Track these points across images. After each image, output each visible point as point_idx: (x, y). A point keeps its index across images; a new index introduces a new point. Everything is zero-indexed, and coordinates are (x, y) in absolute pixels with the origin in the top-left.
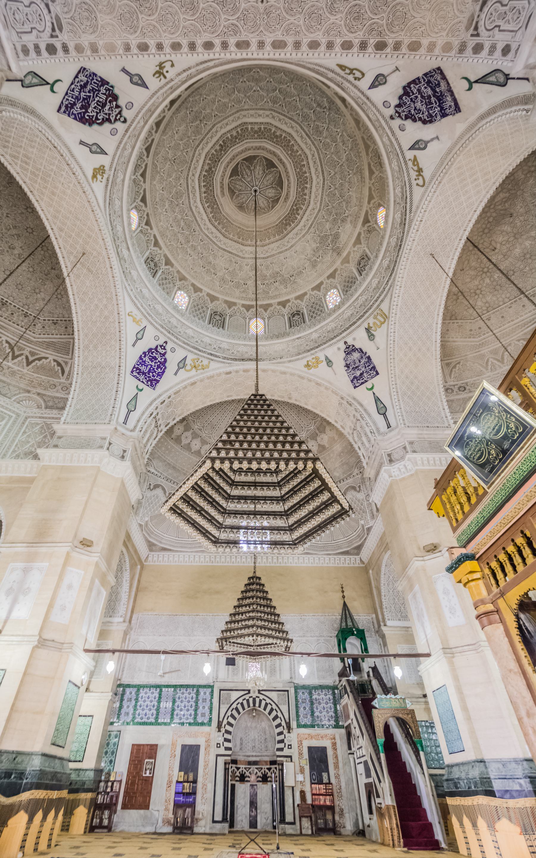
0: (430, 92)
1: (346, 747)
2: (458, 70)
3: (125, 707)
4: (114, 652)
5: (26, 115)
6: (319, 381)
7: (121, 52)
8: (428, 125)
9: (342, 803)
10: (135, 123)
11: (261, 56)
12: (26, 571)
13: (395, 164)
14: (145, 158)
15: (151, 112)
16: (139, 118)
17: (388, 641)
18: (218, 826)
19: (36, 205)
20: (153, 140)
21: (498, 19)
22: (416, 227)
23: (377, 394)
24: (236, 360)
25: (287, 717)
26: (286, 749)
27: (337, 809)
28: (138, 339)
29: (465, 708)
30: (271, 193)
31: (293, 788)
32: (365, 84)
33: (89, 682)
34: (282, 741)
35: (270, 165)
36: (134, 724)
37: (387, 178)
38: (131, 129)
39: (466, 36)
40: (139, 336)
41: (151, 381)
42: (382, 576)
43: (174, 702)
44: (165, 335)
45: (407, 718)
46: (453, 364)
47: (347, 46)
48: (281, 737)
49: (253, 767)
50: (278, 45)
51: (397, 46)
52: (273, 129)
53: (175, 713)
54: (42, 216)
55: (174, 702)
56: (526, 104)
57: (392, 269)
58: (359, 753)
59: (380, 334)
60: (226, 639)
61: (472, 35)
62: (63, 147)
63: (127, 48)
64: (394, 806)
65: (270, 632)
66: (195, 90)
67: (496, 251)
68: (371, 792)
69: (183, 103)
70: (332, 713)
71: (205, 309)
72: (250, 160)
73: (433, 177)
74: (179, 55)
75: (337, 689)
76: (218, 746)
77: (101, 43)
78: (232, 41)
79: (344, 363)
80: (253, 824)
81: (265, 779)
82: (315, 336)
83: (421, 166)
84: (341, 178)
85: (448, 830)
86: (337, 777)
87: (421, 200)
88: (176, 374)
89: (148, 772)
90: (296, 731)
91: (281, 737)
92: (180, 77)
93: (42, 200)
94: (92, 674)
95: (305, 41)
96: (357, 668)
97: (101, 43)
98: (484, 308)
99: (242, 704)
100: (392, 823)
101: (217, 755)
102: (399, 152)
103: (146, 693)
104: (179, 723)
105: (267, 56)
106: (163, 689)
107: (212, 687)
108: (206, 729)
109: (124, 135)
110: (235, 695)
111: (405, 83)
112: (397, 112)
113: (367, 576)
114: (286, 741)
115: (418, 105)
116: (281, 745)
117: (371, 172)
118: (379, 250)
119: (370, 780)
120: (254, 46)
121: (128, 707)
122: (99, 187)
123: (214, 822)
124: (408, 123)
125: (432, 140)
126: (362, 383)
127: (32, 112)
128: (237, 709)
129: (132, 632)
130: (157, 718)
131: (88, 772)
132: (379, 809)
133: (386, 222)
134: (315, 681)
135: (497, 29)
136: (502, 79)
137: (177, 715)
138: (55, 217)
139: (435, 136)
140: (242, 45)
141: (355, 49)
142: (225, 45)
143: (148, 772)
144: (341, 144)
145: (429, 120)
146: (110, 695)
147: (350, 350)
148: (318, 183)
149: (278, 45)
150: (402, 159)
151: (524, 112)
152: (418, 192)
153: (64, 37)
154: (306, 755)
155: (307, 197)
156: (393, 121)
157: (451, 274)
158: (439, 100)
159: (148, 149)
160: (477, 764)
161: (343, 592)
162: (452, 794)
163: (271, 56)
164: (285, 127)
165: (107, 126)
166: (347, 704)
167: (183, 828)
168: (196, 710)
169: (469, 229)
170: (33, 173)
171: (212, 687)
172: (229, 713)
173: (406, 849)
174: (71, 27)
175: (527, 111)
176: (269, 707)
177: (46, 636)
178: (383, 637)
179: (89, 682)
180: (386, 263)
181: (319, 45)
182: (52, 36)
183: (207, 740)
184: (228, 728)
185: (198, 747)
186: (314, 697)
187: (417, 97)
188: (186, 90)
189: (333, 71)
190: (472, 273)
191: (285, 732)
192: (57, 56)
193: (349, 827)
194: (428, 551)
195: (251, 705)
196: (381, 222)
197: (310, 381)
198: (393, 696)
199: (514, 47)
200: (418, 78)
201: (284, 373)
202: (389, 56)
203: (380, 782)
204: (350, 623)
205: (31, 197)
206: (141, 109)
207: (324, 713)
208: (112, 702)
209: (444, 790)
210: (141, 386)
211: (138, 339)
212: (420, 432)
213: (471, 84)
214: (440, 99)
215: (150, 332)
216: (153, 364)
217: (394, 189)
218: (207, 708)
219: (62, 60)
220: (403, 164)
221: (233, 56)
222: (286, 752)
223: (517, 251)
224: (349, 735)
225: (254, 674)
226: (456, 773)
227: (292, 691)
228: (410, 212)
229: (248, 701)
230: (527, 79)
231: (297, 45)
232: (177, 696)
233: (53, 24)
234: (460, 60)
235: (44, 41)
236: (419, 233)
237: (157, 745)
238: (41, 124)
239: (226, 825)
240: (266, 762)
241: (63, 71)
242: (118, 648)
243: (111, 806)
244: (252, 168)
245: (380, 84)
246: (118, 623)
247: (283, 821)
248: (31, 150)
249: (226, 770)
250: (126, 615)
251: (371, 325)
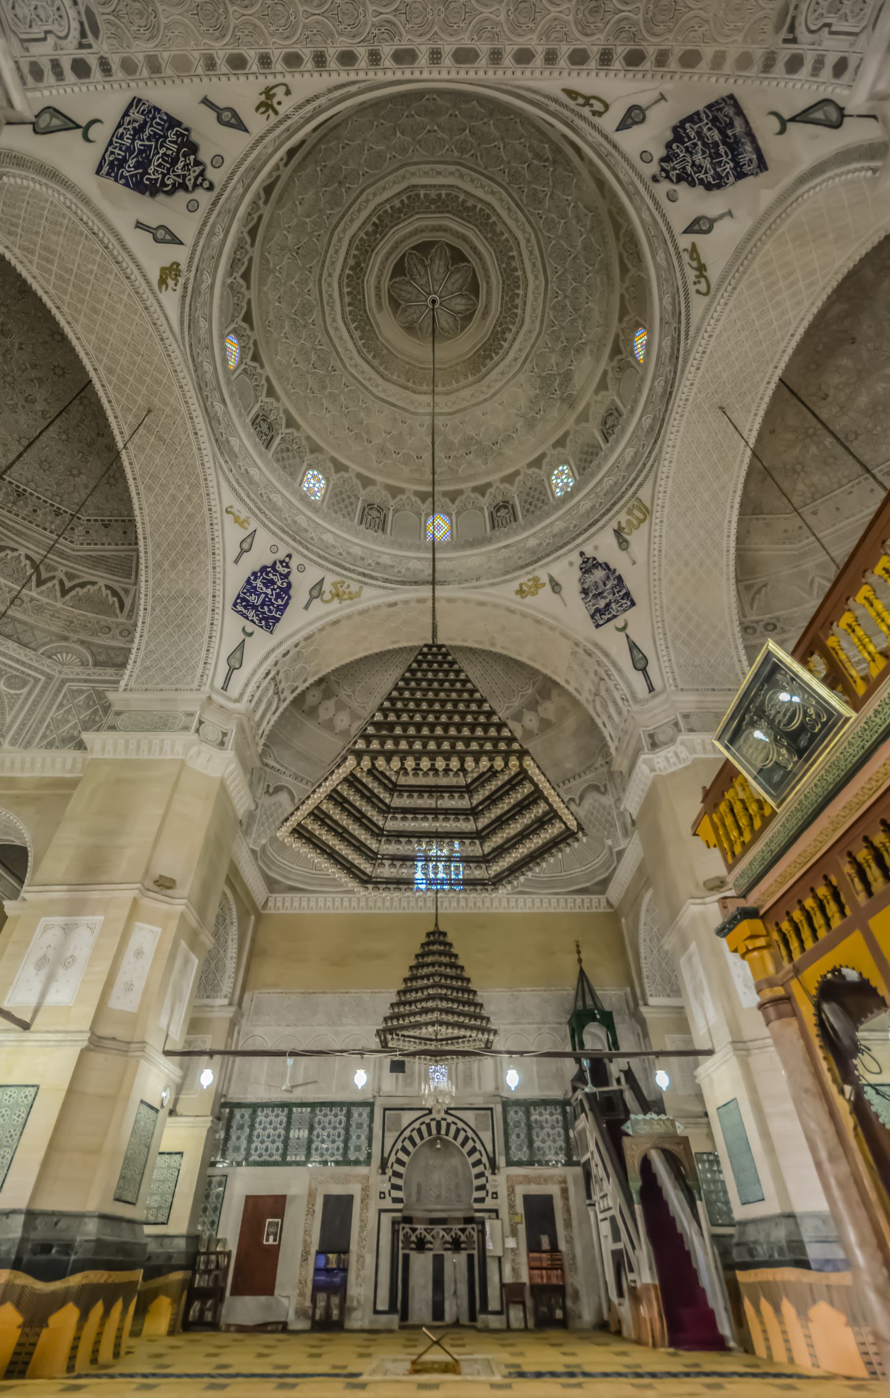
0: (717, 136)
1: (583, 1193)
2: (766, 98)
3: (234, 1138)
4: (211, 1054)
5: (44, 180)
6: (540, 616)
7: (200, 71)
8: (715, 192)
9: (577, 1280)
10: (229, 190)
11: (435, 75)
12: (67, 929)
13: (661, 257)
14: (248, 246)
15: (255, 170)
16: (234, 182)
17: (651, 1030)
18: (384, 1318)
19: (67, 330)
20: (260, 218)
21: (829, 12)
22: (695, 363)
23: (632, 637)
24: (404, 583)
25: (490, 1149)
26: (488, 1200)
27: (569, 1290)
28: (243, 551)
29: (765, 1134)
30: (459, 304)
31: (500, 1259)
32: (610, 121)
33: (176, 1101)
34: (482, 1188)
35: (458, 257)
36: (248, 1165)
37: (649, 281)
38: (221, 201)
39: (775, 41)
40: (246, 546)
41: (266, 619)
42: (642, 927)
43: (311, 1129)
44: (287, 544)
45: (677, 1150)
46: (755, 589)
47: (579, 58)
48: (482, 1181)
49: (438, 1229)
50: (464, 56)
51: (662, 59)
52: (462, 197)
53: (314, 1146)
54: (79, 349)
55: (311, 1129)
56: (873, 158)
57: (656, 431)
58: (603, 1204)
59: (637, 539)
60: (391, 1031)
61: (786, 41)
62: (108, 234)
63: (210, 64)
64: (655, 1286)
65: (461, 1019)
66: (329, 131)
67: (829, 399)
68: (620, 1262)
69: (310, 152)
70: (561, 1143)
71: (353, 499)
72: (424, 248)
73: (723, 279)
74: (297, 76)
75: (570, 1104)
76: (382, 1195)
77: (165, 56)
78: (387, 50)
79: (578, 587)
80: (438, 1312)
81: (456, 1245)
82: (532, 542)
83: (703, 261)
84: (574, 280)
85: (739, 1319)
86: (570, 1241)
87: (703, 318)
88: (306, 607)
89: (271, 1238)
90: (505, 1172)
91: (482, 1181)
92: (302, 112)
93: (77, 321)
94: (179, 1089)
95: (509, 50)
96: (599, 1074)
97: (166, 55)
98: (809, 495)
99: (419, 1131)
100: (651, 1311)
101: (381, 1211)
102: (667, 236)
103: (267, 1116)
104: (320, 1162)
105: (447, 76)
106: (294, 1110)
107: (371, 1105)
108: (363, 1170)
109: (211, 211)
110: (407, 1117)
111: (675, 122)
112: (663, 169)
113: (615, 930)
114: (488, 1187)
115: (698, 158)
116: (482, 1194)
117: (624, 269)
118: (636, 401)
119: (619, 1246)
120: (423, 60)
121: (238, 1138)
122: (170, 300)
123: (376, 1312)
124: (682, 189)
125: (721, 217)
126: (609, 620)
127: (53, 175)
128: (411, 1139)
129: (244, 1021)
130: (284, 1155)
131: (176, 1241)
132: (633, 1290)
133: (648, 354)
134: (535, 1093)
135: (826, 29)
136: (834, 116)
137: (317, 1149)
138: (100, 350)
139: (725, 210)
140: (405, 57)
141: (593, 64)
142: (375, 58)
143: (271, 1238)
144: (574, 222)
145: (716, 184)
146: (208, 1121)
147: (589, 565)
148: (537, 288)
149: (464, 56)
150: (672, 250)
151: (870, 173)
152: (698, 304)
153: (102, 46)
154: (520, 1208)
155: (519, 311)
156: (657, 185)
157: (752, 441)
158: (733, 150)
159: (253, 233)
160: (784, 1220)
161: (579, 952)
162: (746, 1266)
163: (453, 75)
164: (479, 190)
165: (181, 197)
166: (584, 1129)
167: (328, 1325)
168: (346, 1142)
169: (782, 365)
170: (60, 277)
171: (371, 1105)
172: (399, 1145)
173: (672, 1350)
174: (113, 30)
175: (874, 170)
176: (462, 1135)
177: (105, 1031)
178: (642, 1022)
179: (176, 1101)
180: (647, 422)
181: (533, 56)
182: (81, 46)
183: (365, 1185)
184: (398, 1168)
185: (350, 1198)
186: (533, 1118)
187: (695, 145)
188: (315, 130)
189: (556, 101)
190: (789, 436)
191: (488, 1173)
192: (92, 79)
193: (588, 1316)
194: (712, 889)
195: (434, 1132)
196: (640, 353)
197: (524, 615)
198: (655, 1116)
199: (852, 63)
200: (697, 113)
201: (482, 604)
202: (649, 76)
203: (634, 1248)
204: (589, 1002)
205: (59, 317)
206: (238, 166)
207: (549, 1141)
208: (212, 1131)
209: (735, 1257)
210: (250, 627)
211: (243, 551)
212: (701, 698)
213: (783, 123)
214: (734, 147)
215: (264, 540)
216: (269, 591)
217: (661, 299)
218: (363, 1137)
219: (100, 87)
220: (674, 258)
221: (390, 76)
222: (489, 1203)
223: (863, 400)
224: (588, 1175)
225: (438, 1082)
226: (752, 1234)
227: (498, 1109)
228: (686, 338)
229: (428, 1126)
230: (874, 117)
231: (496, 56)
232: (317, 1119)
233: (81, 24)
234: (766, 83)
235: (69, 53)
236: (700, 372)
237: (284, 1197)
238: (68, 195)
239: (395, 1318)
240: (457, 1220)
241: (103, 103)
242: (221, 1048)
243: (215, 1294)
244: (427, 262)
245: (636, 123)
246: (220, 1008)
247: (484, 1309)
248: (54, 238)
249: (395, 1233)
250: (233, 994)
251: (623, 525)
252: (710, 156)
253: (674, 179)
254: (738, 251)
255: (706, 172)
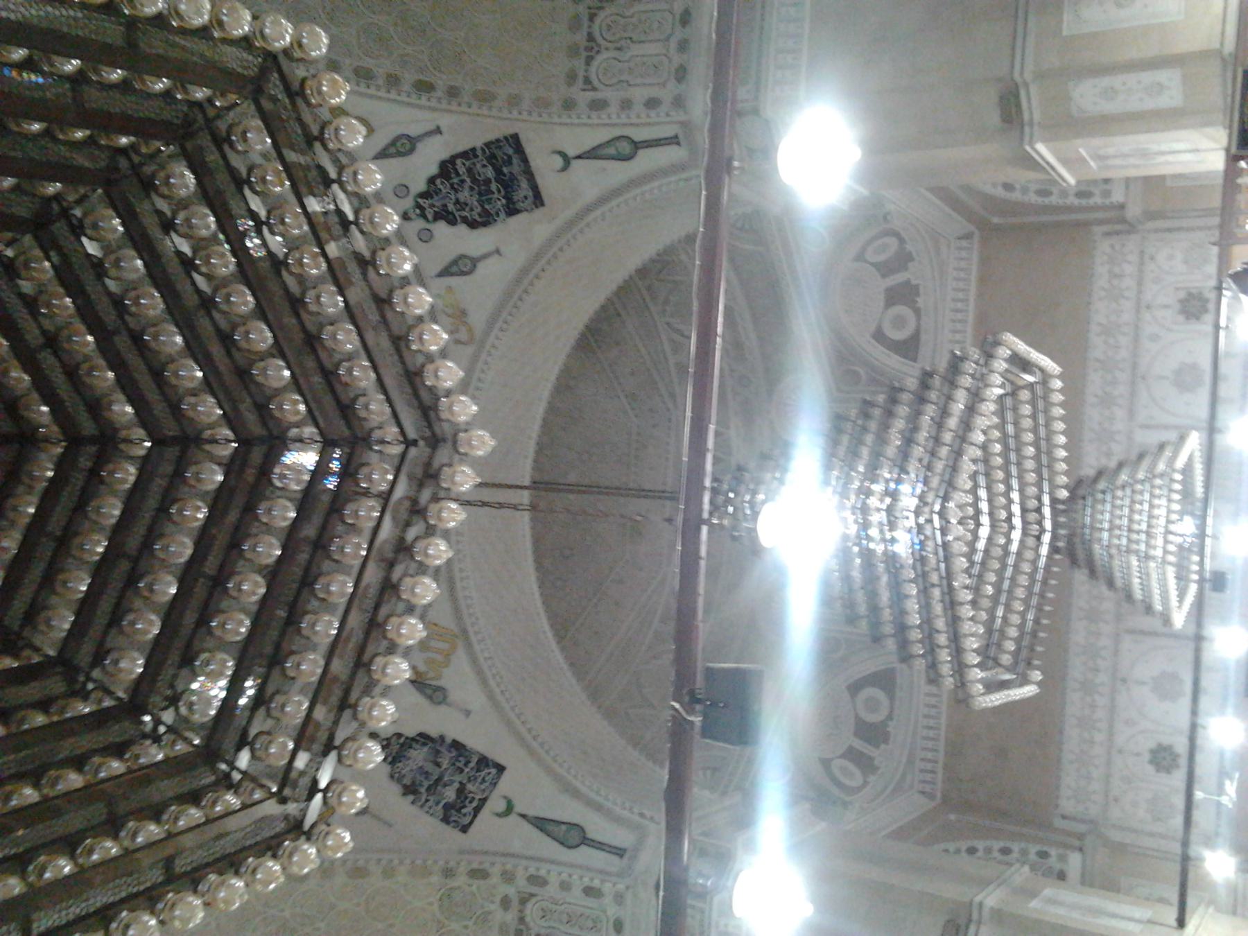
0: (490, 172)
23: (531, 813)
115: (464, 195)
124: (441, 228)
145: (484, 220)
158: (506, 187)
187: (463, 181)
214: (508, 185)
252: (480, 194)
253: (430, 217)
254: (508, 295)
255: (472, 210)
